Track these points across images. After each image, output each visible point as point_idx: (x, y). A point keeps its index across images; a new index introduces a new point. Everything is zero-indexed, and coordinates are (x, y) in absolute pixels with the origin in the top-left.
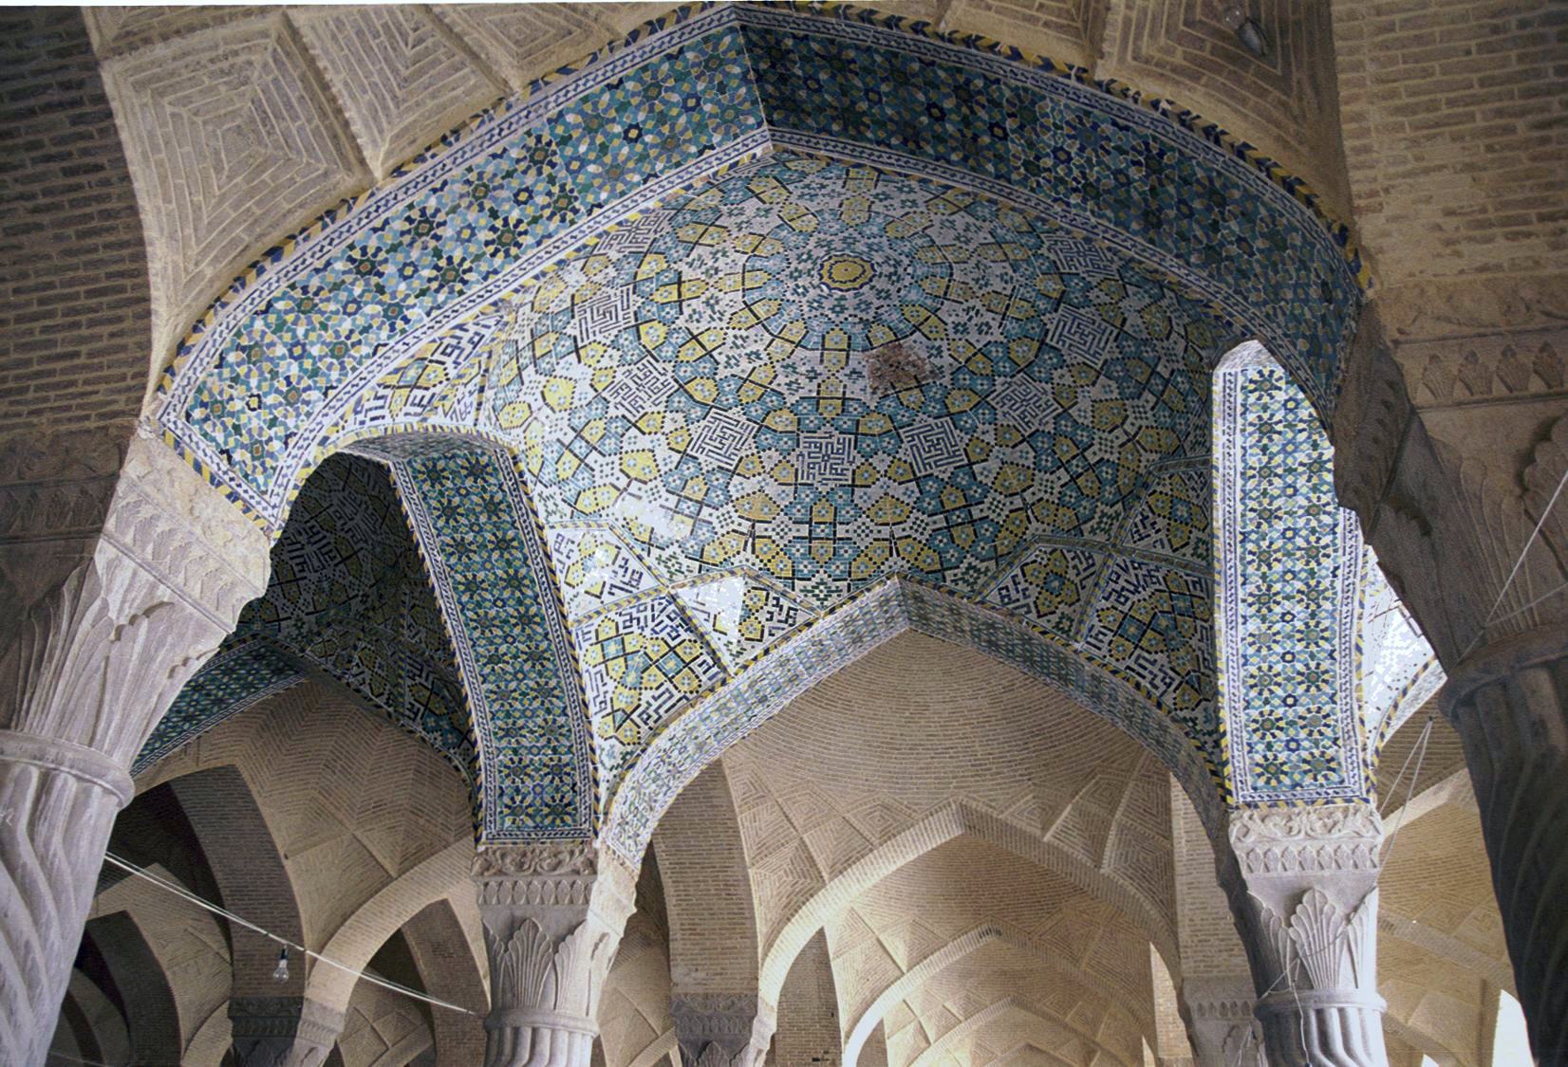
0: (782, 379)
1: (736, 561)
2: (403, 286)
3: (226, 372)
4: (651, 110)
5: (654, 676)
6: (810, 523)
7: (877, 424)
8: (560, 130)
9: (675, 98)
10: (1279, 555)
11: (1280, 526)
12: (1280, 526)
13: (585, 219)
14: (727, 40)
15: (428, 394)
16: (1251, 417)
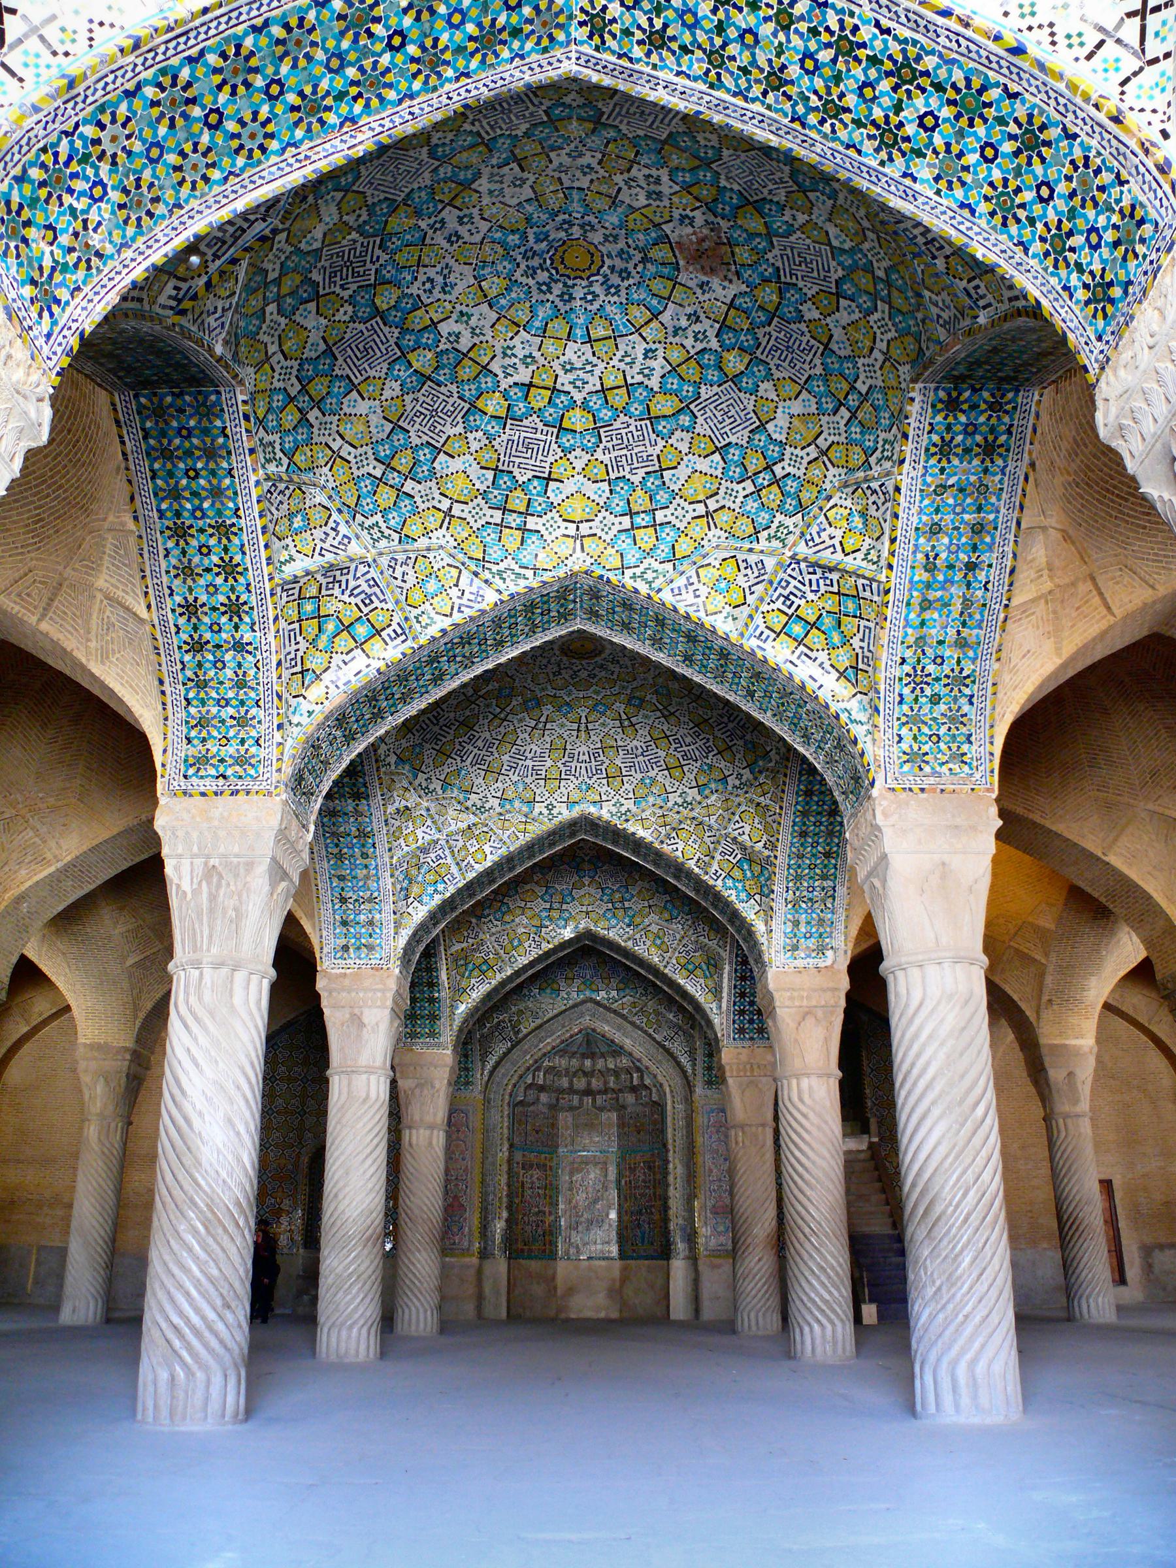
0: (689, 343)
1: (828, 486)
2: (224, 635)
3: (195, 742)
4: (180, 458)
5: (849, 624)
6: (841, 404)
7: (769, 295)
8: (169, 514)
9: (177, 441)
10: (835, 92)
11: (794, 71)
12: (794, 71)
13: (243, 521)
14: (143, 400)
15: (395, 626)
16: (638, 52)
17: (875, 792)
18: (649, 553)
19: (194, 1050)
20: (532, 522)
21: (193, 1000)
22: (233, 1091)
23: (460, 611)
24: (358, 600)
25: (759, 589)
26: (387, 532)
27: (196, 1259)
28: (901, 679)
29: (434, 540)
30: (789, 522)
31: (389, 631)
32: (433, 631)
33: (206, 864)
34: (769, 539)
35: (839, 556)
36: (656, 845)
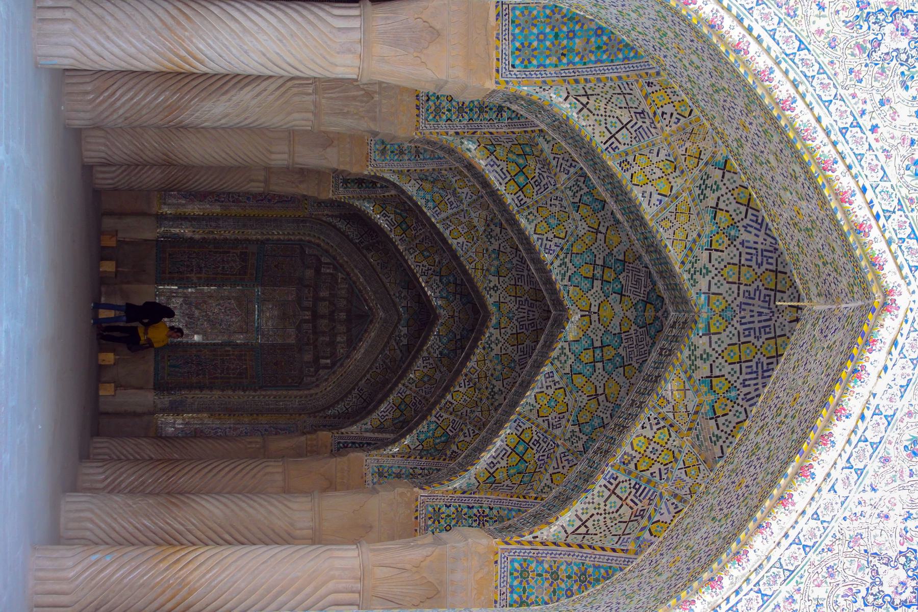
5: (517, 479)
17: (416, 489)
18: (578, 358)
19: (265, 93)
20: (597, 283)
21: (295, 90)
22: (243, 116)
23: (538, 239)
24: (537, 178)
25: (545, 425)
26: (578, 195)
27: (151, 102)
28: (481, 507)
29: (580, 223)
30: (580, 444)
31: (522, 196)
32: (523, 222)
33: (375, 92)
34: (573, 431)
35: (551, 471)
36: (464, 371)
